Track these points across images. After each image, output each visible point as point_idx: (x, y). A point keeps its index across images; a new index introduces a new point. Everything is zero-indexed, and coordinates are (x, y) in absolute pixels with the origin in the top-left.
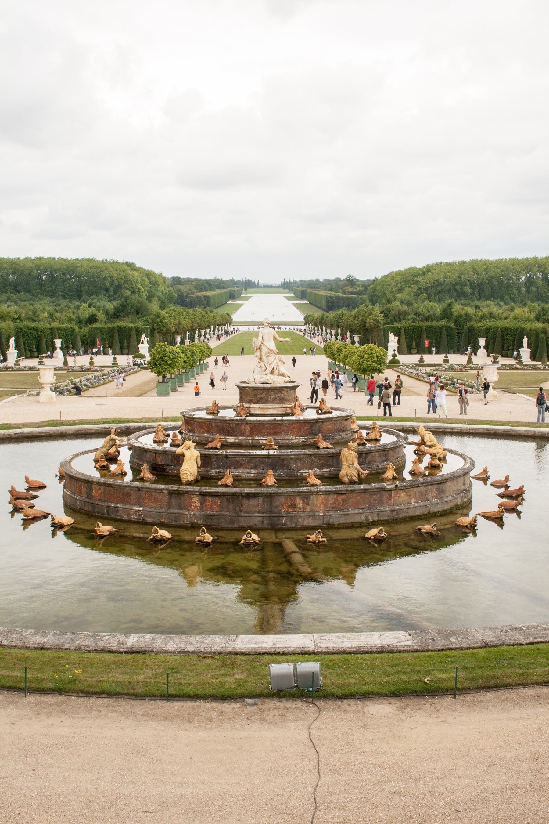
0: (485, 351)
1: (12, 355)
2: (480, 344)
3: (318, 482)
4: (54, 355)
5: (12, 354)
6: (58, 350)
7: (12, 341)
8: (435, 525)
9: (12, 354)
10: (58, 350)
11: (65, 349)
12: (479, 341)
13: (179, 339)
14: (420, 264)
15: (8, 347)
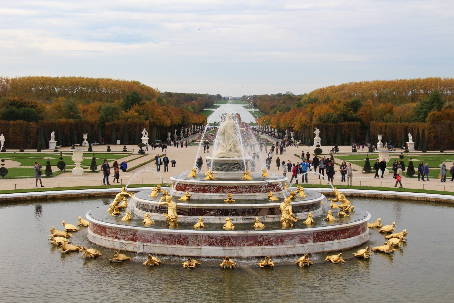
0: (382, 143)
1: (53, 144)
2: (379, 139)
3: (262, 226)
4: (83, 144)
5: (53, 143)
6: (85, 141)
7: (53, 134)
8: (341, 255)
9: (53, 143)
10: (85, 141)
11: (90, 141)
12: (377, 136)
13: (170, 134)
14: (337, 83)
15: (50, 138)
